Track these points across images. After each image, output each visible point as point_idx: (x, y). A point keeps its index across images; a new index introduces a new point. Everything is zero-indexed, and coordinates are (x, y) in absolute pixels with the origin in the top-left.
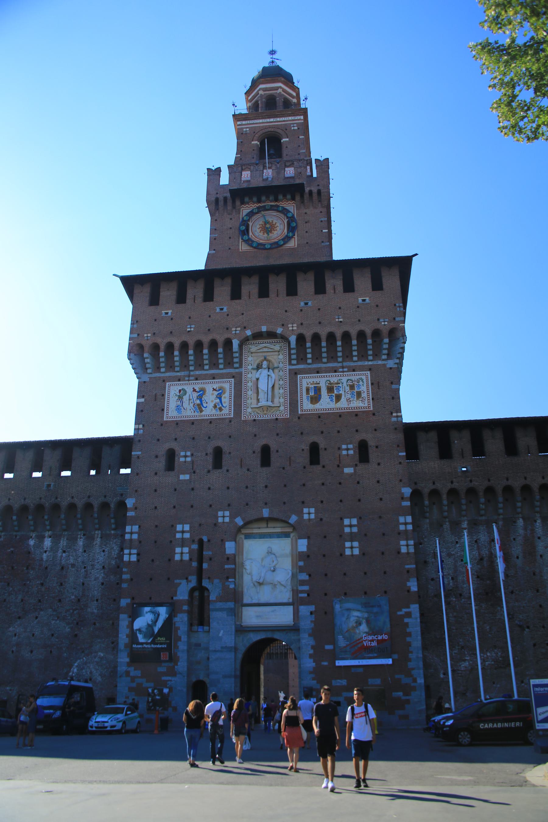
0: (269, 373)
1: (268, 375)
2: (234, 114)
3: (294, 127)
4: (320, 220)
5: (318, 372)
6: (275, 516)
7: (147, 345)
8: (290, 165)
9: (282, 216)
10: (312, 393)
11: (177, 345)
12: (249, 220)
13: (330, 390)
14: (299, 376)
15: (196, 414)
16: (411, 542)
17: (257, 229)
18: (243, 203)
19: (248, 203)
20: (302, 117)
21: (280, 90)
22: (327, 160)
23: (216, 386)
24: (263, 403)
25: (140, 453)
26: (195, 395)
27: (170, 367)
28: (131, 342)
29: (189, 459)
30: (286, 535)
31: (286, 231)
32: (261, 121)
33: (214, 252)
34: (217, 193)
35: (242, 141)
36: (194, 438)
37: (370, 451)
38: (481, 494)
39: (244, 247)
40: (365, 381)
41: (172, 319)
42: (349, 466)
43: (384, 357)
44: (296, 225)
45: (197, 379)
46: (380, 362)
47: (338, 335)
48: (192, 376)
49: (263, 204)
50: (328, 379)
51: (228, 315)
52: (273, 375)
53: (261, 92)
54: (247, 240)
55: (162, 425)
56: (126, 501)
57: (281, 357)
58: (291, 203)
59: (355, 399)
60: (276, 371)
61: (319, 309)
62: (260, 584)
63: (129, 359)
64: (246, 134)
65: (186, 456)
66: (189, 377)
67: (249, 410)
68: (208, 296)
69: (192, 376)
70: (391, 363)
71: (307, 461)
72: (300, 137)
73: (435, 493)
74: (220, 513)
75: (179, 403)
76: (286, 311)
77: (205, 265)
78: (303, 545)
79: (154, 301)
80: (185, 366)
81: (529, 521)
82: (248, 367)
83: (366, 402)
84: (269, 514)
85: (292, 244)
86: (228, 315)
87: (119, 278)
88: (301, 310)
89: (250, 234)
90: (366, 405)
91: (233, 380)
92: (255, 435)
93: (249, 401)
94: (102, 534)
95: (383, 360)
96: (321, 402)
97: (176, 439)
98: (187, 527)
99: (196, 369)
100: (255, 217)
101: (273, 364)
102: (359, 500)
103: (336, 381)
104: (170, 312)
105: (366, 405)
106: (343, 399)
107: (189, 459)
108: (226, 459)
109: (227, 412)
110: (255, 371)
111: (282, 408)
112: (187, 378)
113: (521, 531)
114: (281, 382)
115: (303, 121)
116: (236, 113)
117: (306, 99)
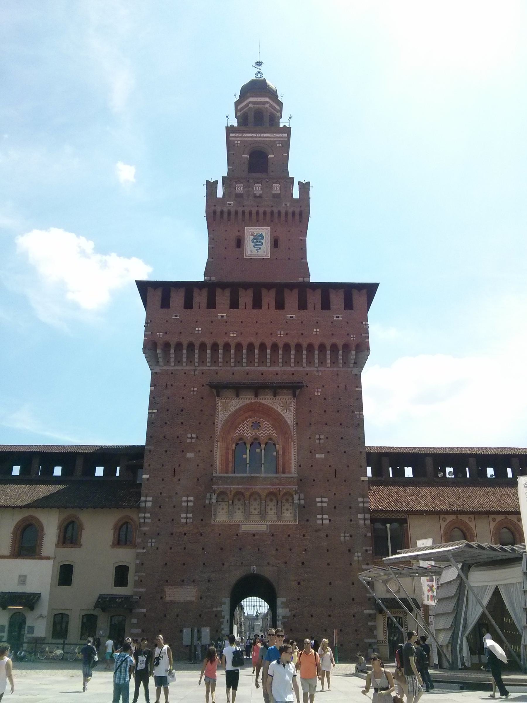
2: (227, 126)
3: (279, 144)
4: (300, 238)
20: (286, 135)
21: (267, 106)
22: (308, 183)
28: (146, 338)
33: (212, 260)
35: (233, 152)
43: (352, 365)
53: (250, 105)
64: (237, 146)
66: (195, 371)
68: (211, 304)
72: (284, 155)
79: (165, 303)
116: (229, 126)
117: (290, 118)
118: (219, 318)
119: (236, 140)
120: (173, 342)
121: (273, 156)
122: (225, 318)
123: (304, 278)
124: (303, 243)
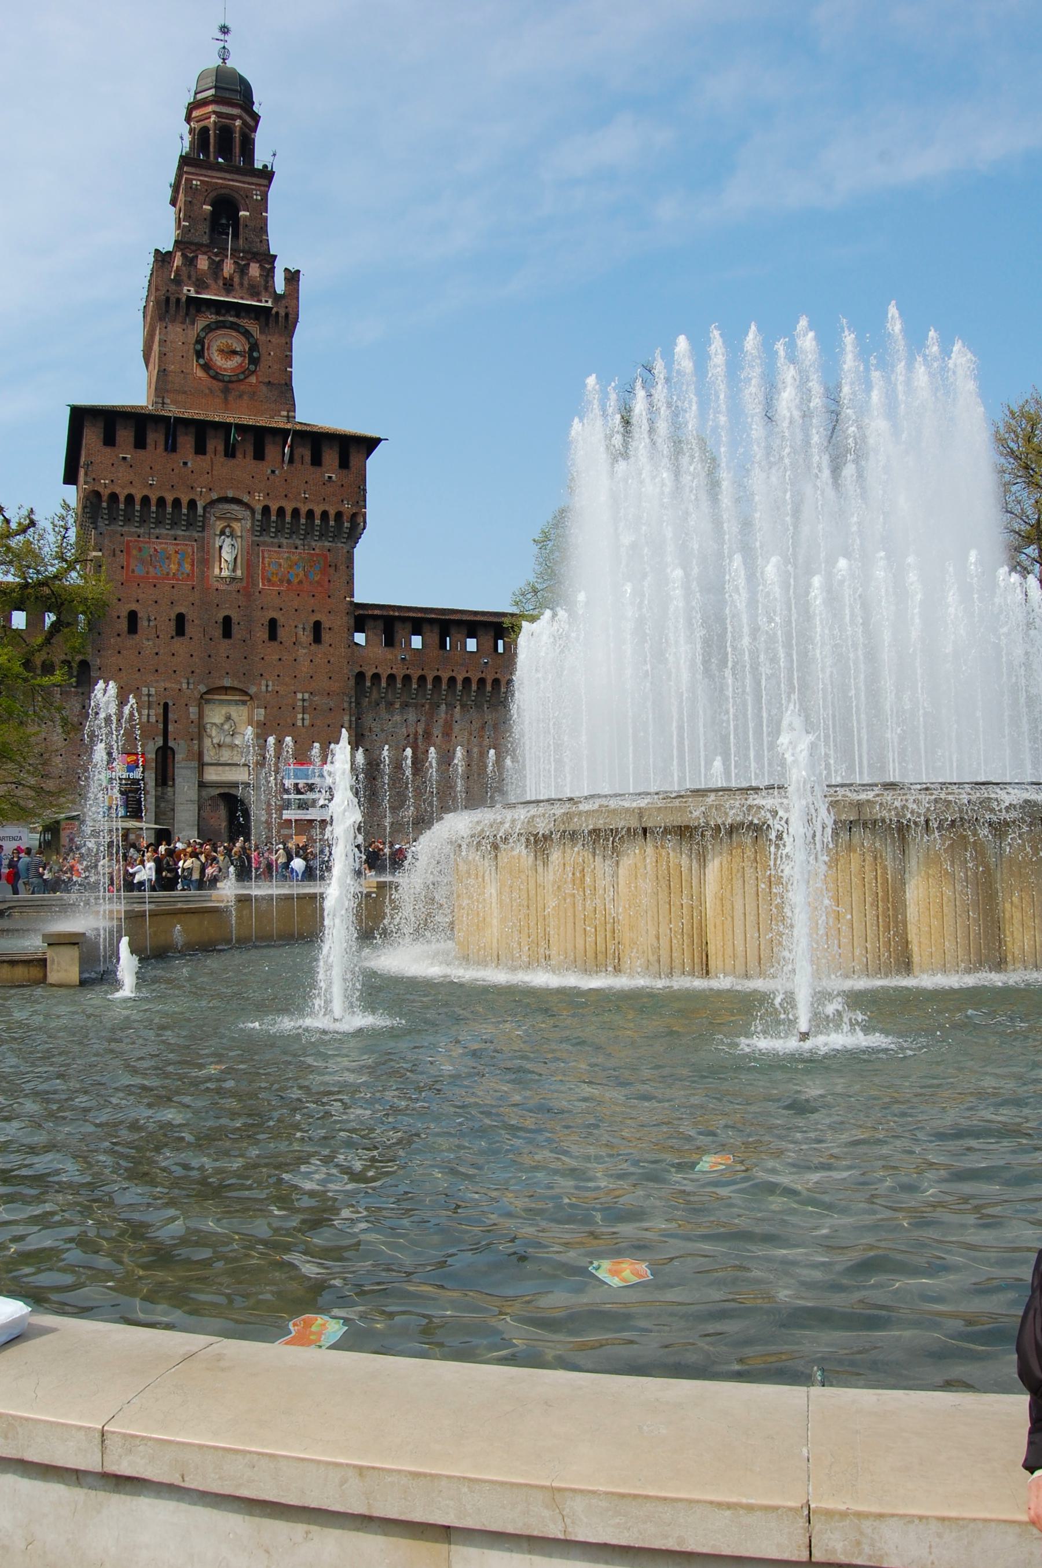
1: (233, 545)
3: (257, 195)
7: (105, 493)
8: (252, 258)
9: (243, 340)
11: (138, 498)
12: (204, 338)
16: (353, 719)
18: (198, 311)
19: (204, 312)
22: (298, 272)
24: (225, 573)
29: (152, 624)
30: (244, 703)
34: (168, 291)
35: (189, 199)
36: (156, 602)
38: (414, 681)
39: (200, 373)
44: (259, 358)
47: (304, 510)
49: (221, 318)
51: (192, 472)
55: (122, 584)
60: (239, 540)
62: (219, 745)
64: (197, 189)
71: (266, 636)
73: (376, 677)
78: (260, 714)
79: (109, 440)
81: (451, 706)
85: (253, 379)
86: (192, 472)
94: (61, 691)
97: (138, 601)
100: (211, 335)
102: (311, 677)
113: (443, 715)
116: (184, 154)
117: (274, 155)
119: (192, 180)
122: (189, 464)
123: (288, 412)
124: (288, 361)
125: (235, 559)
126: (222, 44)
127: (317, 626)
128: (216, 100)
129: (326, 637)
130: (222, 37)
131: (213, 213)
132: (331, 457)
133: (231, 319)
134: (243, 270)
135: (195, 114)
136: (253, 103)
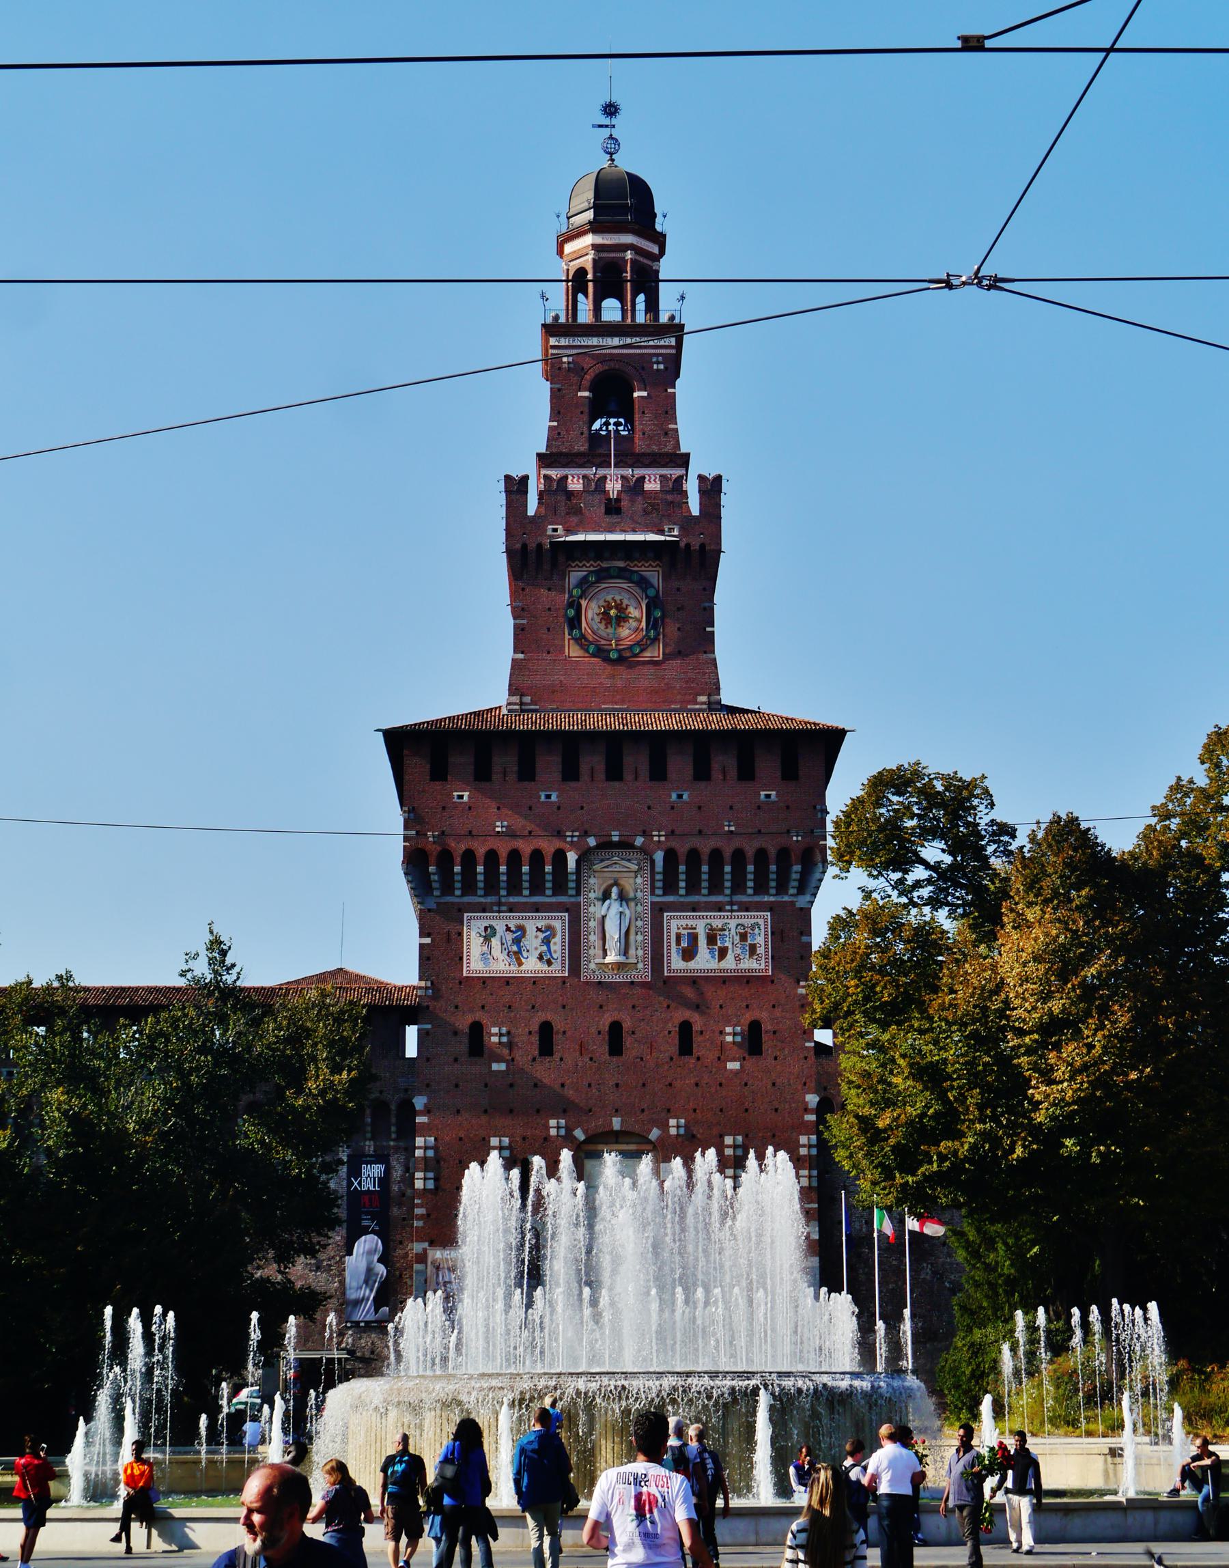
0: (621, 909)
3: (658, 363)
5: (694, 910)
6: (630, 1129)
7: (434, 850)
9: (637, 591)
10: (684, 944)
13: (711, 939)
14: (665, 914)
15: (513, 968)
16: (815, 1173)
17: (595, 616)
22: (718, 479)
23: (541, 924)
24: (611, 958)
25: (429, 1026)
26: (510, 937)
27: (469, 886)
31: (644, 624)
32: (594, 341)
33: (521, 656)
37: (764, 1037)
39: (574, 651)
40: (762, 927)
41: (470, 808)
42: (734, 1060)
45: (511, 911)
46: (786, 898)
47: (727, 854)
48: (504, 904)
49: (605, 565)
50: (709, 921)
51: (559, 808)
52: (627, 912)
54: (580, 639)
55: (460, 983)
56: (414, 1101)
57: (639, 880)
58: (654, 564)
59: (747, 956)
60: (632, 904)
61: (700, 808)
63: (405, 874)
65: (501, 1035)
67: (592, 966)
69: (504, 904)
70: (801, 901)
71: (674, 1049)
74: (553, 1123)
75: (485, 948)
76: (649, 808)
77: (510, 685)
80: (492, 886)
82: (590, 895)
83: (763, 962)
84: (622, 1126)
87: (381, 734)
88: (673, 808)
89: (584, 624)
90: (763, 967)
91: (566, 914)
92: (601, 1007)
93: (591, 952)
95: (792, 895)
96: (697, 958)
97: (483, 1007)
98: (506, 1141)
99: (509, 895)
101: (628, 893)
102: (747, 1110)
103: (720, 926)
104: (466, 794)
105: (763, 967)
106: (730, 956)
107: (504, 1039)
108: (557, 1039)
109: (558, 969)
110: (600, 903)
111: (640, 966)
112: (495, 908)
114: (639, 923)
115: (674, 351)
117: (683, 297)
118: (543, 798)
120: (459, 848)
121: (645, 394)
122: (554, 798)
123: (709, 695)
125: (627, 933)
126: (606, 132)
127: (755, 1029)
128: (595, 227)
129: (767, 1042)
130: (607, 121)
131: (591, 401)
132: (767, 765)
133: (621, 564)
134: (634, 488)
135: (569, 248)
136: (655, 215)
